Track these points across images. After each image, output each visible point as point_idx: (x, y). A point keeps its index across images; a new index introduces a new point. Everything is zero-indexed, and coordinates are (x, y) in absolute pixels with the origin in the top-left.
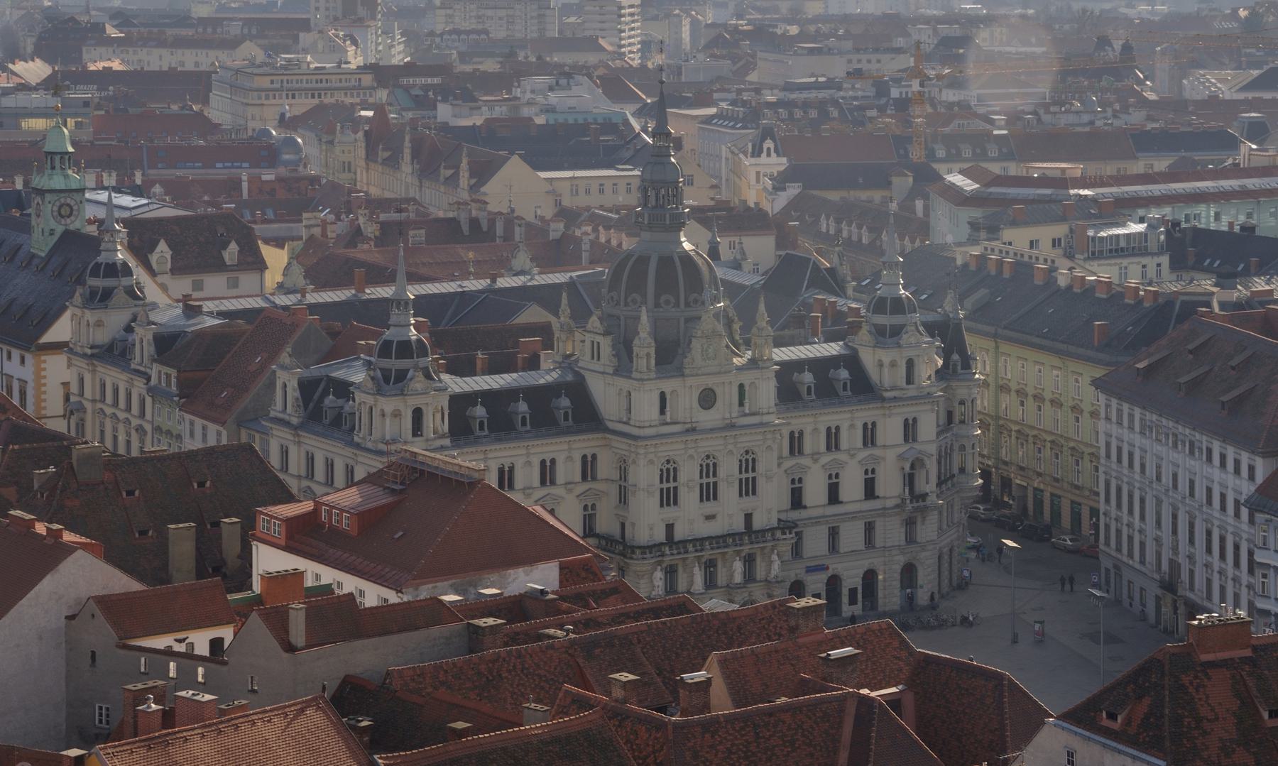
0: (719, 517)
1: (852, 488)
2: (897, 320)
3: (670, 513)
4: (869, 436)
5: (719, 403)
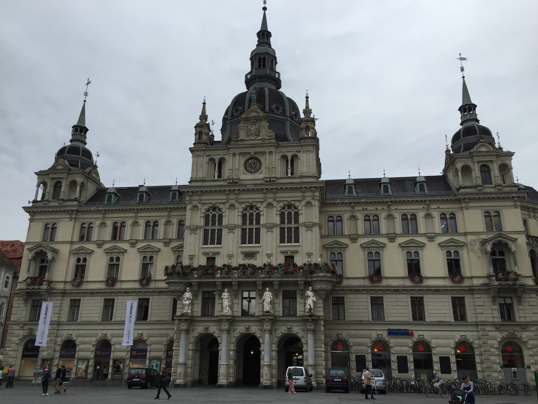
0: (258, 256)
1: (434, 265)
2: (471, 139)
5: (263, 168)
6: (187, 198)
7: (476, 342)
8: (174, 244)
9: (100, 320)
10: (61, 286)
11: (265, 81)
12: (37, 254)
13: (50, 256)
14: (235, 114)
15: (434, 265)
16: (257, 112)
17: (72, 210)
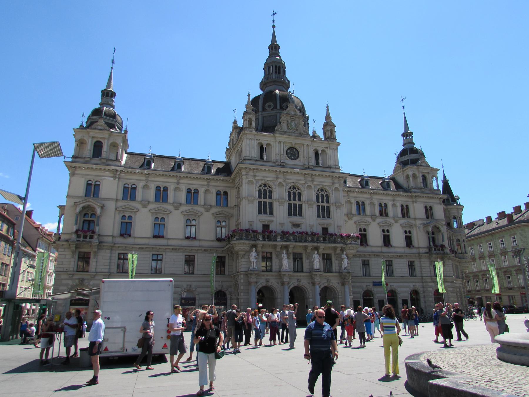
1: (398, 238)
2: (414, 156)
3: (266, 218)
4: (405, 212)
5: (301, 157)
6: (244, 173)
7: (422, 289)
8: (214, 210)
9: (150, 272)
10: (110, 239)
11: (282, 86)
12: (84, 208)
13: (98, 211)
14: (267, 108)
15: (398, 238)
16: (295, 111)
17: (117, 171)
